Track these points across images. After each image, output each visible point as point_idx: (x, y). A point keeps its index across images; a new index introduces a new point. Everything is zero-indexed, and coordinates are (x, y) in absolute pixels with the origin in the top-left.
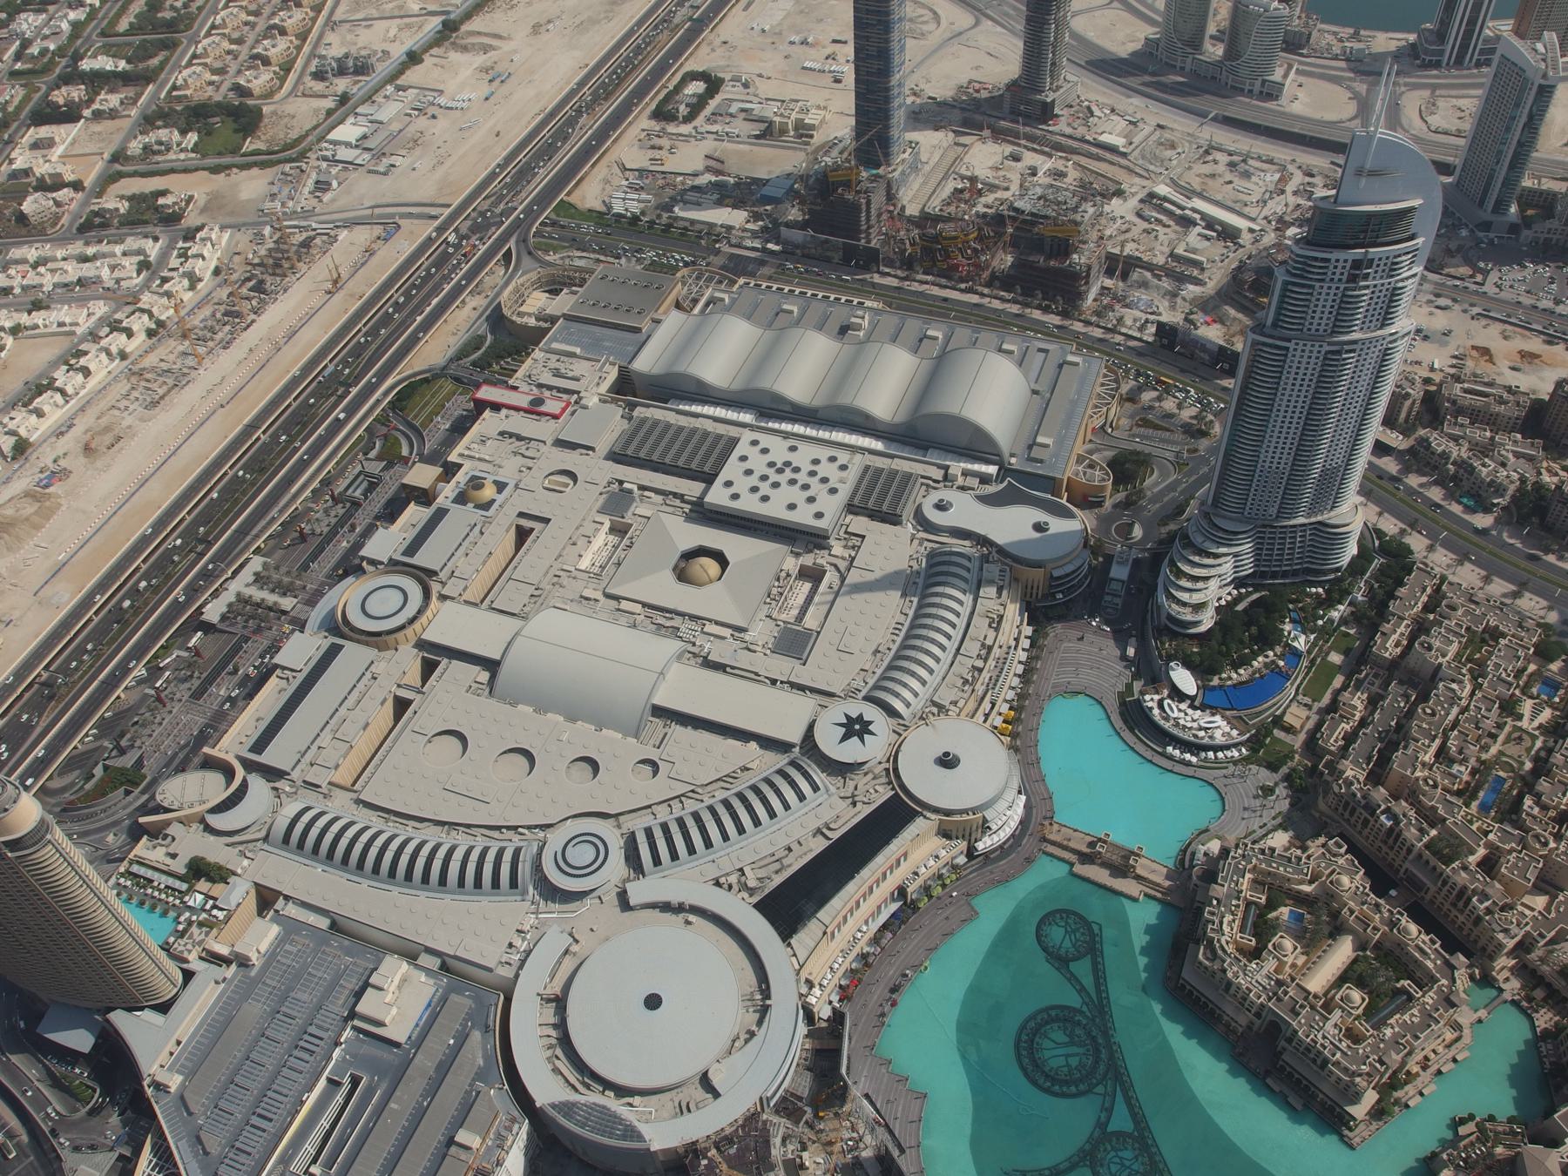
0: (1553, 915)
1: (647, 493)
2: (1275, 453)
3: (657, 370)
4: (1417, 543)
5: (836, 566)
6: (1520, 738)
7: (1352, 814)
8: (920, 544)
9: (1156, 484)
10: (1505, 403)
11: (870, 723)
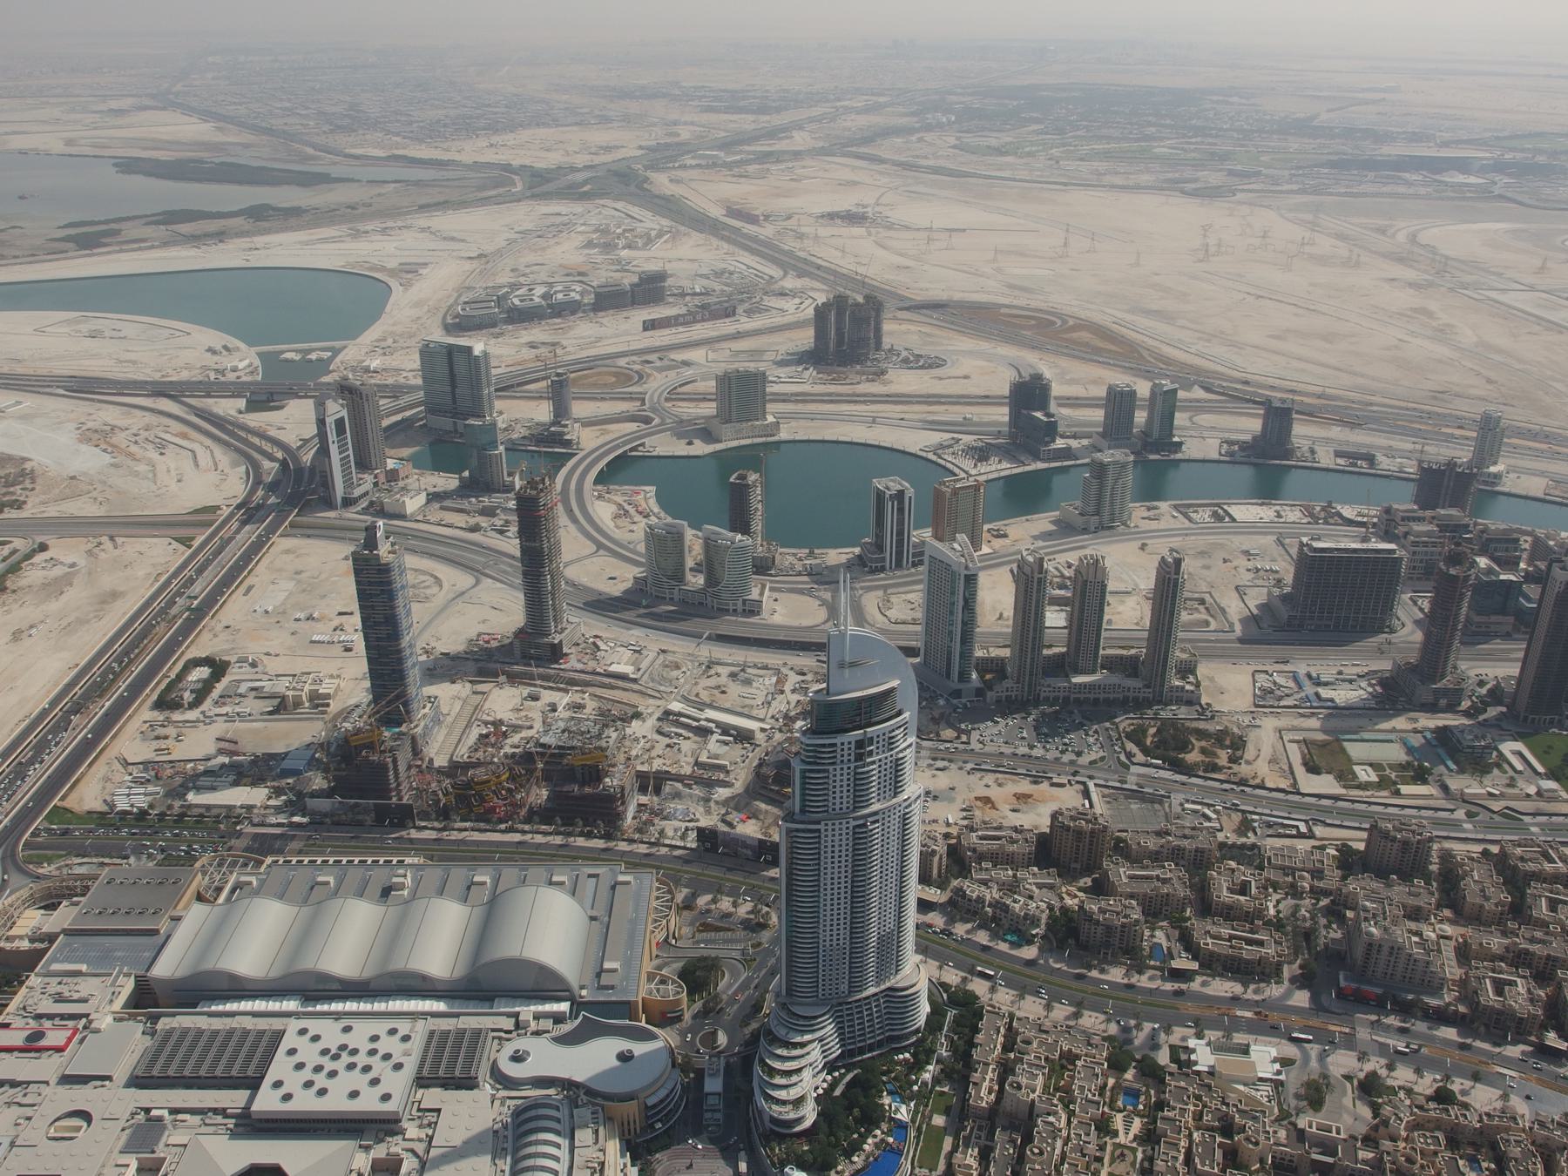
1: (180, 1117)
2: (832, 932)
3: (179, 974)
4: (979, 987)
5: (413, 1151)
6: (1122, 1155)
8: (503, 1104)
9: (730, 985)
10: (1016, 842)
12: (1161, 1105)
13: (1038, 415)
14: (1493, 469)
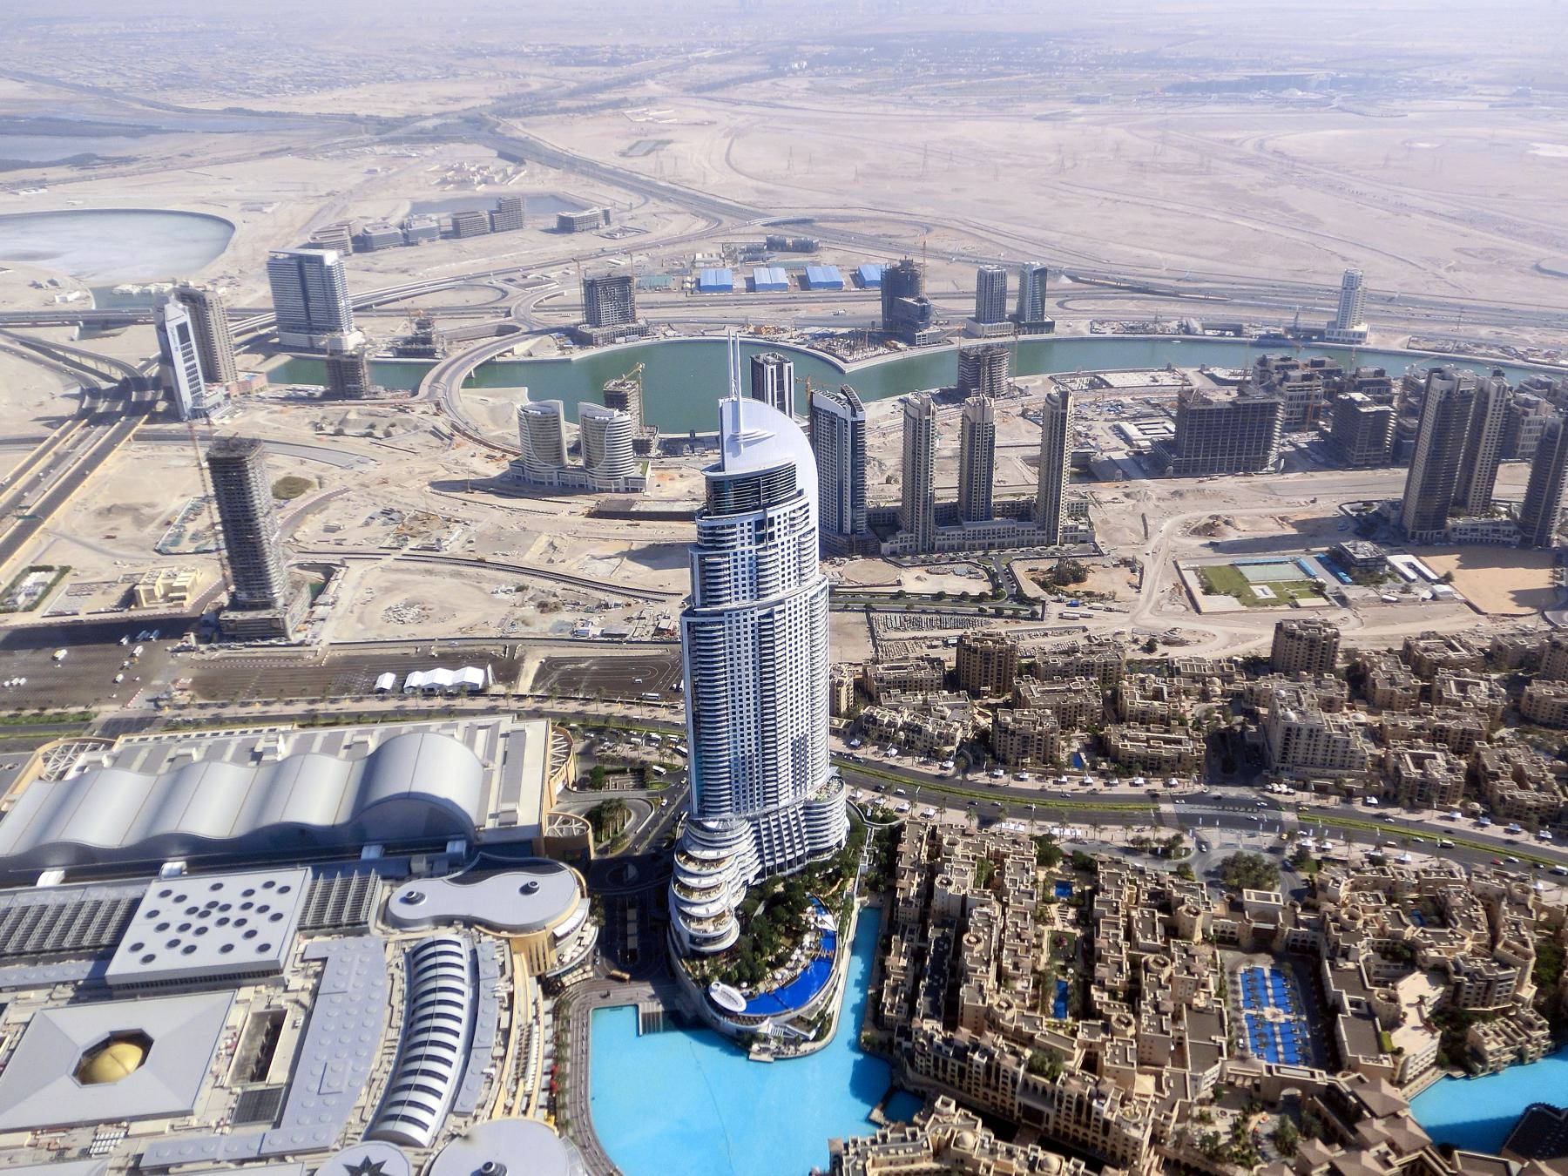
0: (1167, 1093)
1: (21, 994)
5: (297, 1002)
7: (945, 1071)
9: (637, 824)
11: (380, 1165)
12: (1095, 891)
13: (911, 301)
14: (1357, 329)
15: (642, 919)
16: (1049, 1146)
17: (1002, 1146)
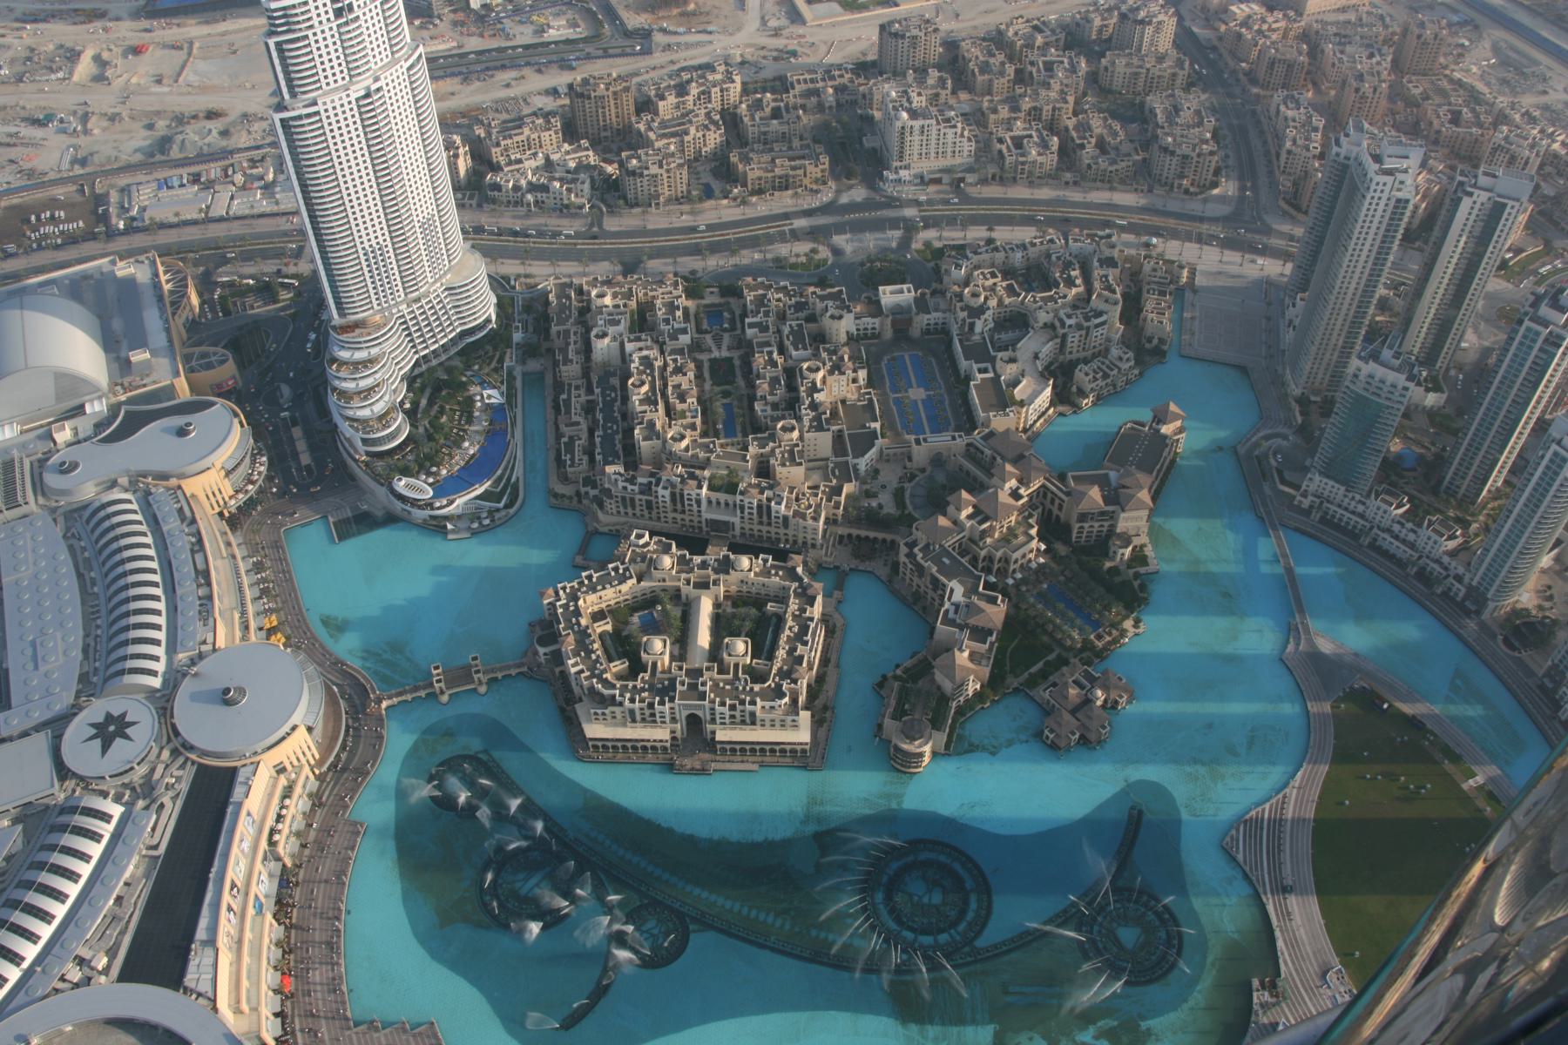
7: (633, 507)
11: (124, 715)
12: (744, 315)
15: (308, 435)
16: (738, 549)
17: (698, 559)
